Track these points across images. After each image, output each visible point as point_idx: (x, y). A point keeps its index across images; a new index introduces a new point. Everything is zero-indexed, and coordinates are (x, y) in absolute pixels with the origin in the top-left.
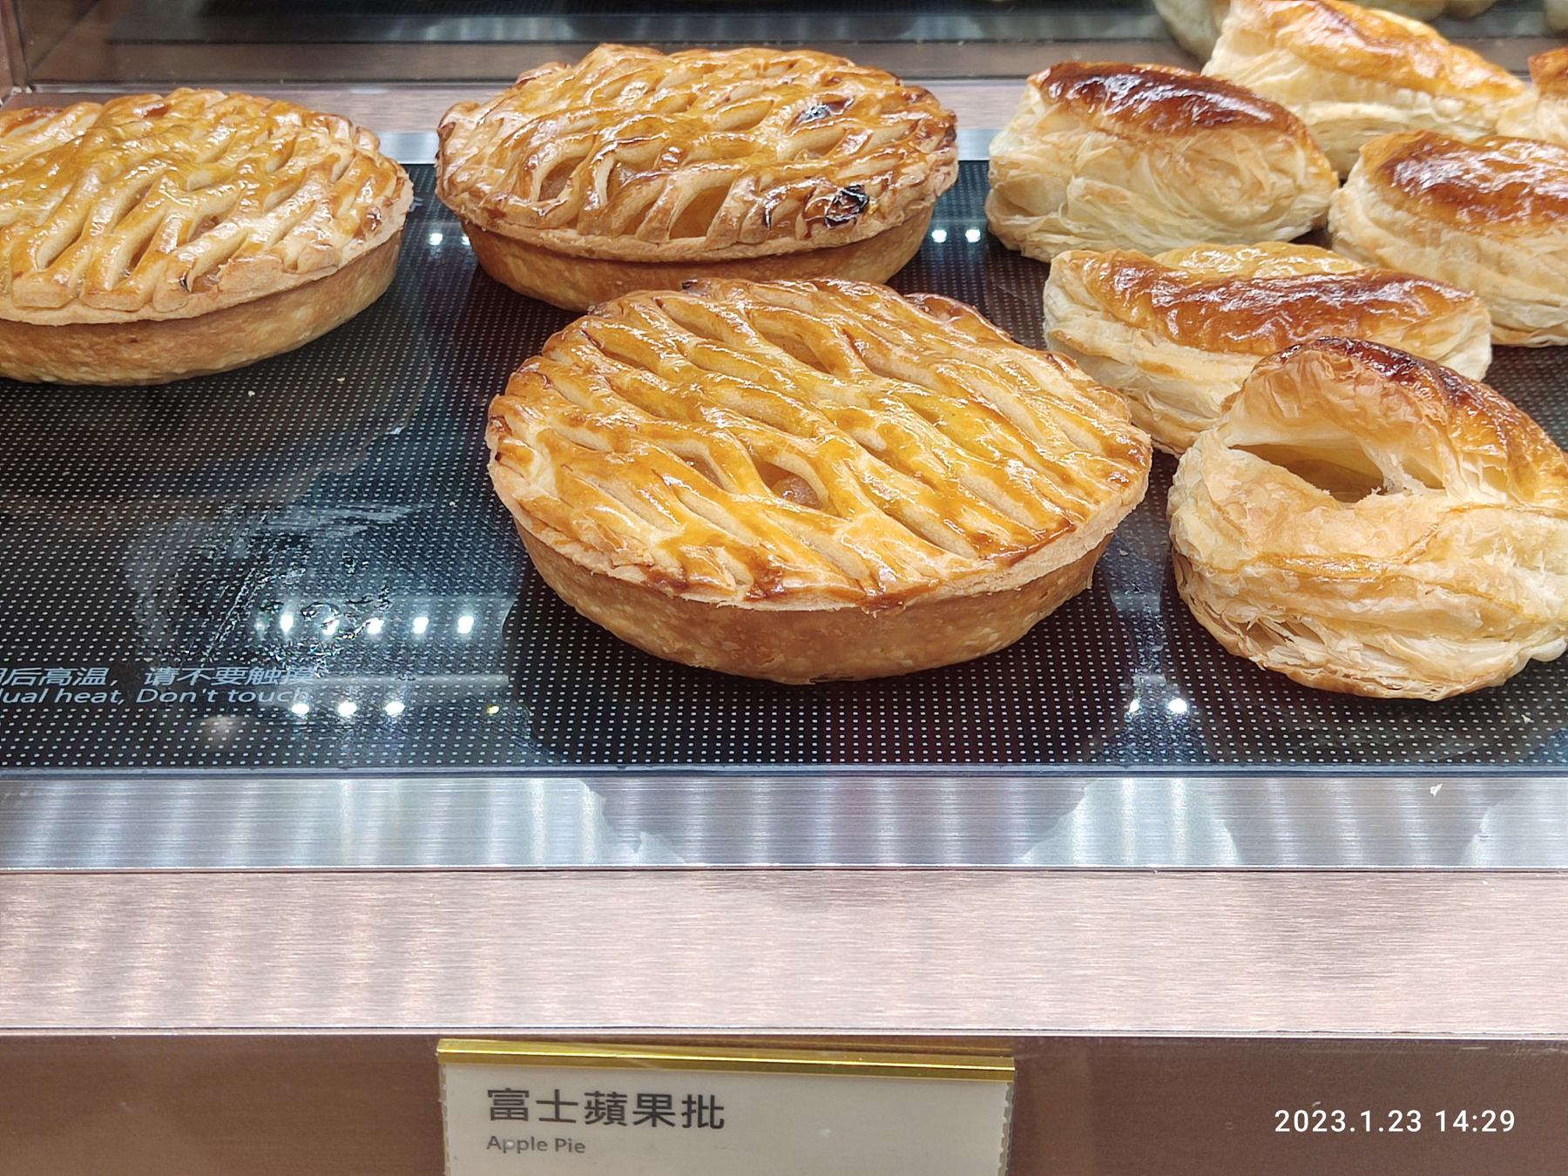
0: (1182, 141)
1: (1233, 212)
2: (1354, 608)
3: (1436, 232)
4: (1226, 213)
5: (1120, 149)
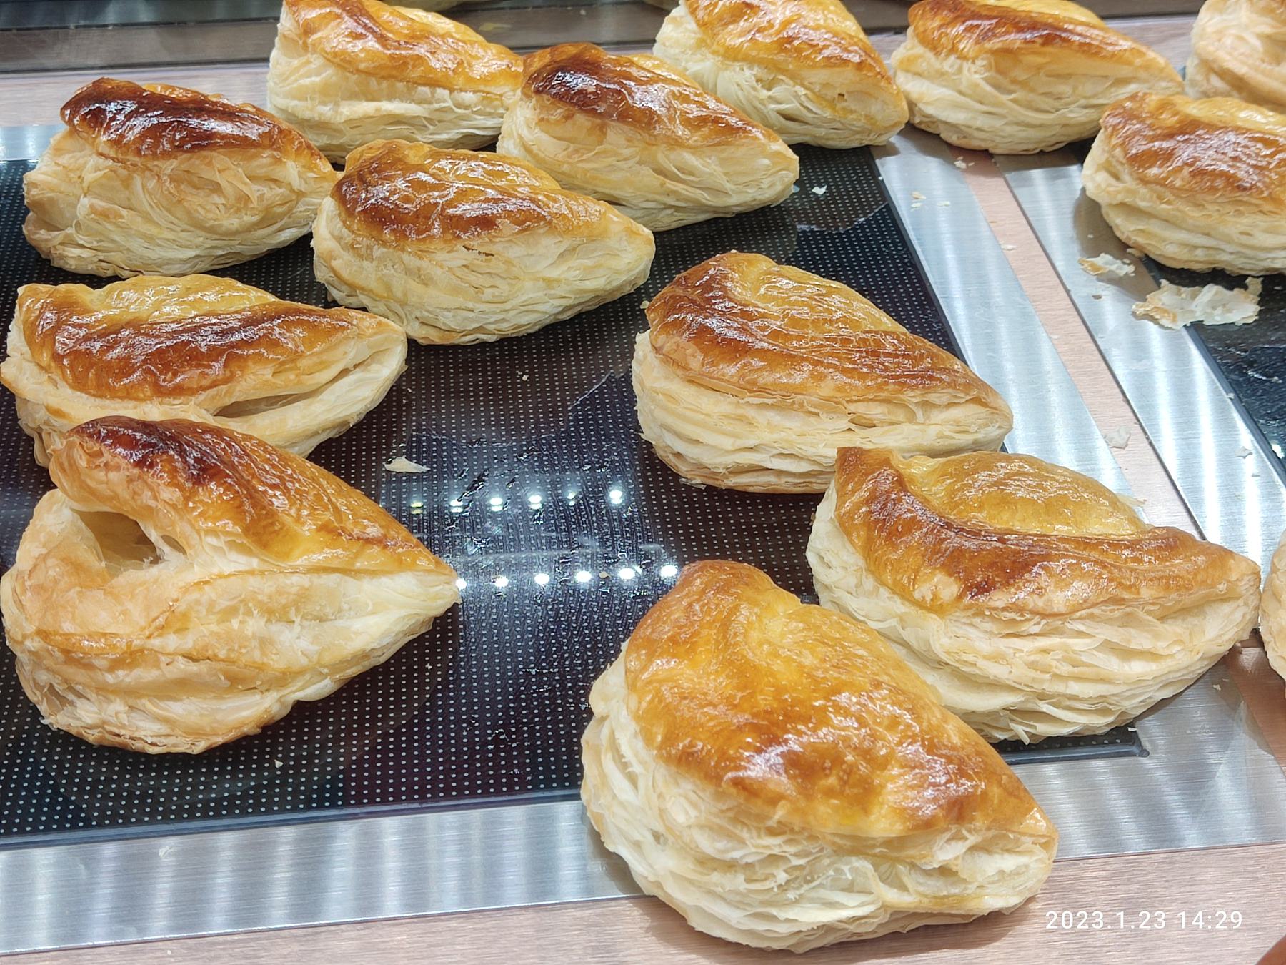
0: (169, 163)
1: (220, 226)
2: (110, 678)
3: (369, 248)
4: (212, 226)
5: (114, 171)
